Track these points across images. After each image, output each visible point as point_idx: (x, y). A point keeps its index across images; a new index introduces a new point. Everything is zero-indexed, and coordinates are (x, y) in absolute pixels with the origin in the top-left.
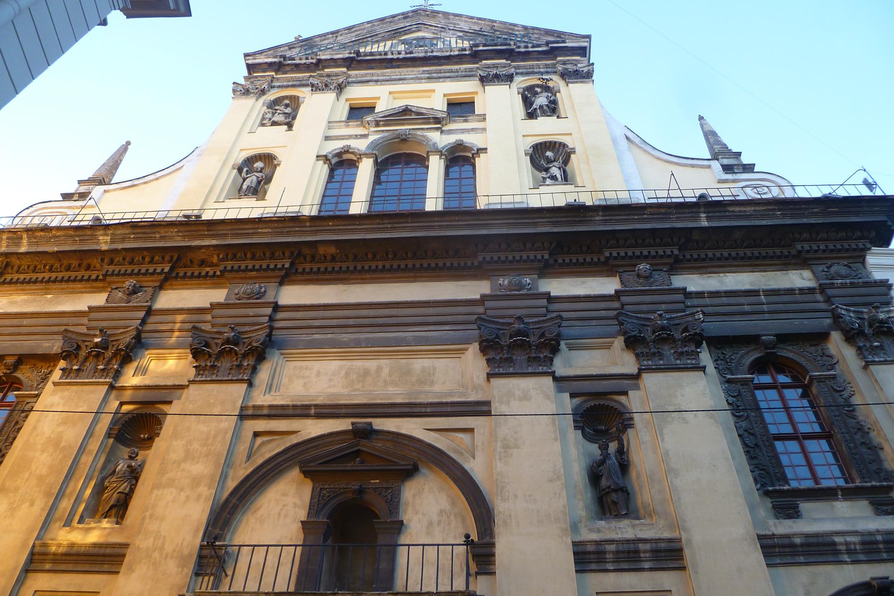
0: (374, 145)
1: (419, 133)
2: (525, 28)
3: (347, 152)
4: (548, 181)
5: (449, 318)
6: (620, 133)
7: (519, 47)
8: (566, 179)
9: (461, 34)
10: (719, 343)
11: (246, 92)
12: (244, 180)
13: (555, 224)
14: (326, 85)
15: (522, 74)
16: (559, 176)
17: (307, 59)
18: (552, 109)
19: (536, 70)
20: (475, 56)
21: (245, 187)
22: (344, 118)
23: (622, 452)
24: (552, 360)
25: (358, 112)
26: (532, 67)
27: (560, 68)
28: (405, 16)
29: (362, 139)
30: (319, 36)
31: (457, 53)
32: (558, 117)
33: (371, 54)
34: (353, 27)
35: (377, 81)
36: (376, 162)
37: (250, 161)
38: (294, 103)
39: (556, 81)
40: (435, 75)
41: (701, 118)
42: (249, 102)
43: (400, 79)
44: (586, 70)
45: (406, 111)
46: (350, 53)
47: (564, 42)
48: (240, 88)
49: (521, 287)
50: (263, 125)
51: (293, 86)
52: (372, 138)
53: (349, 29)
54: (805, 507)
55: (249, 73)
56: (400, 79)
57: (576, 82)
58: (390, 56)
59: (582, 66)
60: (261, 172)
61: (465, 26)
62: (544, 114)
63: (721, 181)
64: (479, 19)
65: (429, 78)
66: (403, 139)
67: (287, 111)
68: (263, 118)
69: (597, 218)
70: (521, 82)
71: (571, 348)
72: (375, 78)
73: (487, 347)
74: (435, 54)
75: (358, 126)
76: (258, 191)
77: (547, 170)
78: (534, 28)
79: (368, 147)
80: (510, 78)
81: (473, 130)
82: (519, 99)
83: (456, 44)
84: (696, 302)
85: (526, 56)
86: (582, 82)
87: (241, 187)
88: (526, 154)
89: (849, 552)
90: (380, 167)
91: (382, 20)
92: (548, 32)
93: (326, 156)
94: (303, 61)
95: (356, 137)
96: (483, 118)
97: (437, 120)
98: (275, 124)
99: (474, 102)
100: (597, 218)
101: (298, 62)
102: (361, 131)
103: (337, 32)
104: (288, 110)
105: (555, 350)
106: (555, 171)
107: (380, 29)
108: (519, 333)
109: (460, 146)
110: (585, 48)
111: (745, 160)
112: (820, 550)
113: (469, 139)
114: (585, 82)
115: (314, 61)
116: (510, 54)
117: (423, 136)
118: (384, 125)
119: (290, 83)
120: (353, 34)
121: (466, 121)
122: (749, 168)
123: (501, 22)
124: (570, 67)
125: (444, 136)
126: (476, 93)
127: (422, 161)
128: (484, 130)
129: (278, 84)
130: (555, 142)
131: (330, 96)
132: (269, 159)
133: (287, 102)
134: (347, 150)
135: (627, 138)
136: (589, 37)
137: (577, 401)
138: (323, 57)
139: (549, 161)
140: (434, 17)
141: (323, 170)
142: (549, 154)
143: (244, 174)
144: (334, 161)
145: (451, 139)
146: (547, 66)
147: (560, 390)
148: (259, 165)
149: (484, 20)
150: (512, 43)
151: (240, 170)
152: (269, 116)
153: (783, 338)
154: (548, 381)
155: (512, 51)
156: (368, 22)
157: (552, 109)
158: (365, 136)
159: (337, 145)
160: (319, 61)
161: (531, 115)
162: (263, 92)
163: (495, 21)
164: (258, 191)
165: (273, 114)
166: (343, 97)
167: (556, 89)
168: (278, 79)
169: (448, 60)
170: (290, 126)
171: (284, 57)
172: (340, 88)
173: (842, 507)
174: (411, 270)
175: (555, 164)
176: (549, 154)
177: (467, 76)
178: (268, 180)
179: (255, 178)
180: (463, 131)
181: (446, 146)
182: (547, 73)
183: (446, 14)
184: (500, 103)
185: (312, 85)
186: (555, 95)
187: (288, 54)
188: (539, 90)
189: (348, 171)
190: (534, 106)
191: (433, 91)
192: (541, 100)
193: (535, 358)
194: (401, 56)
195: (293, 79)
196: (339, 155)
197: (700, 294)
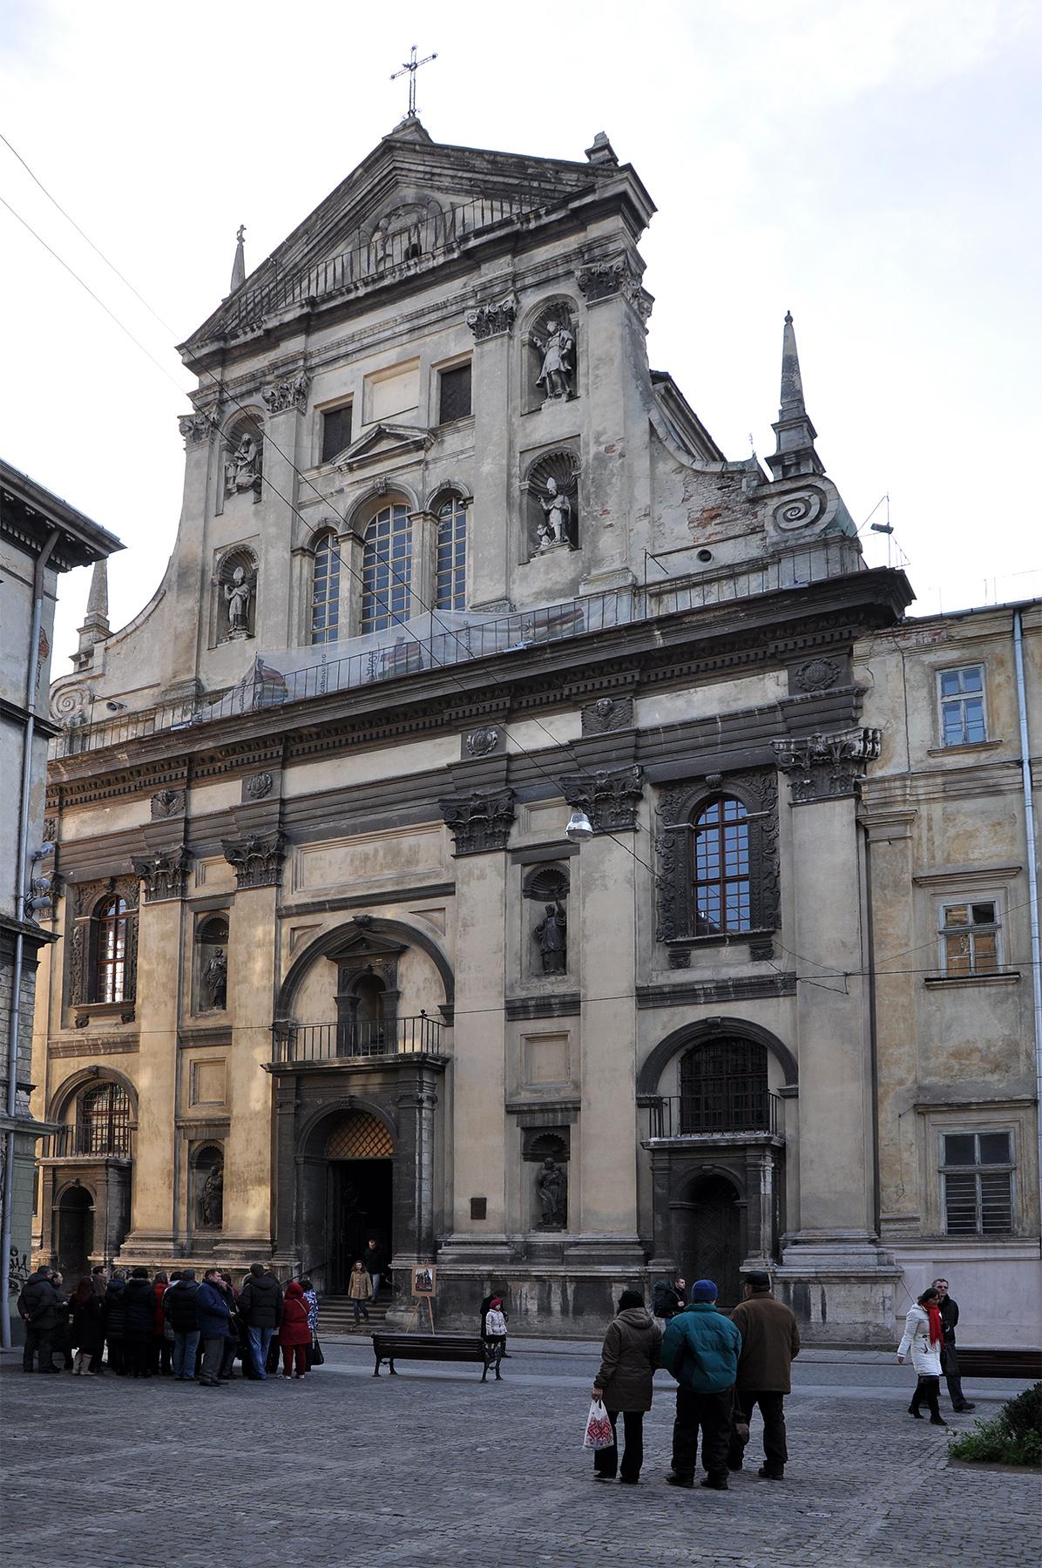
4: (545, 541)
5: (425, 792)
10: (663, 786)
23: (562, 914)
24: (507, 834)
28: (369, 165)
49: (484, 745)
54: (696, 954)
71: (531, 809)
73: (452, 826)
74: (412, 272)
84: (650, 740)
89: (705, 995)
97: (419, 446)
105: (510, 820)
106: (556, 519)
108: (475, 811)
112: (685, 995)
137: (528, 869)
145: (435, 479)
147: (514, 862)
153: (726, 774)
154: (501, 856)
173: (726, 952)
174: (391, 735)
175: (558, 502)
193: (492, 834)
197: (655, 730)
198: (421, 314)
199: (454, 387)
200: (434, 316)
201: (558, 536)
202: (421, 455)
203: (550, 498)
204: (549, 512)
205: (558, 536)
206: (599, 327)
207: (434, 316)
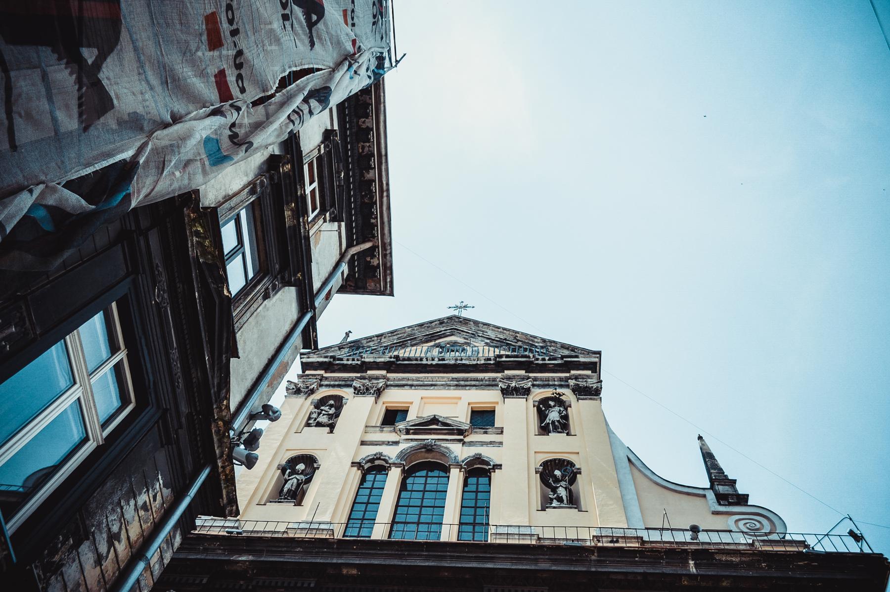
0: (402, 455)
1: (444, 444)
2: (544, 341)
3: (379, 459)
4: (555, 503)
6: (622, 455)
7: (537, 359)
8: (573, 501)
9: (488, 341)
11: (298, 391)
12: (286, 481)
13: (554, 561)
14: (367, 389)
15: (538, 386)
16: (564, 498)
17: (353, 360)
18: (563, 426)
19: (551, 383)
20: (499, 366)
21: (285, 490)
22: (379, 424)
25: (392, 417)
26: (548, 379)
27: (572, 382)
28: (441, 322)
29: (394, 446)
30: (366, 338)
31: (483, 362)
32: (568, 434)
33: (409, 359)
34: (396, 331)
35: (411, 386)
36: (403, 471)
37: (293, 462)
38: (338, 403)
39: (568, 395)
40: (462, 383)
41: (700, 438)
42: (299, 400)
43: (432, 385)
44: (595, 386)
45: (434, 420)
46: (391, 357)
47: (577, 357)
48: (292, 386)
50: (308, 425)
51: (339, 386)
52: (403, 446)
53: (392, 332)
55: (304, 372)
56: (432, 385)
57: (586, 399)
58: (424, 362)
59: (592, 383)
60: (301, 473)
61: (492, 335)
62: (555, 429)
63: (716, 513)
64: (504, 329)
65: (457, 385)
66: (429, 449)
67: (331, 412)
68: (309, 418)
69: (593, 558)
70: (539, 394)
72: (410, 383)
74: (464, 362)
75: (391, 432)
76: (297, 496)
77: (554, 490)
78: (551, 342)
79: (398, 457)
80: (526, 392)
81: (491, 443)
82: (533, 412)
83: (484, 352)
85: (543, 368)
86: (591, 399)
87: (282, 490)
88: (536, 472)
90: (407, 473)
91: (421, 325)
92: (564, 346)
93: (359, 463)
94: (350, 362)
95: (388, 443)
96: (501, 431)
97: (461, 432)
98: (319, 425)
99: (494, 411)
100: (593, 558)
101: (345, 362)
102: (393, 437)
103: (381, 335)
104: (332, 411)
106: (562, 492)
107: (419, 334)
109: (478, 459)
110: (596, 363)
111: (741, 489)
113: (487, 453)
114: (594, 399)
115: (359, 363)
116: (529, 366)
117: (446, 448)
118: (414, 434)
119: (337, 383)
120: (395, 337)
121: (486, 433)
122: (743, 500)
123: (523, 334)
124: (582, 384)
125: (465, 448)
126: (497, 403)
127: (446, 469)
128: (501, 443)
129: (326, 383)
130: (564, 460)
131: (370, 399)
132: (310, 461)
133: (332, 402)
134: (379, 457)
135: (629, 460)
136: (599, 353)
138: (367, 360)
139: (557, 480)
140: (466, 324)
141: (357, 474)
142: (557, 473)
143: (286, 476)
144: (366, 467)
146: (561, 379)
148: (301, 467)
149: (509, 330)
150: (531, 355)
151: (283, 470)
152: (315, 416)
155: (532, 362)
156: (409, 327)
157: (563, 426)
158: (396, 443)
159: (370, 451)
160: (363, 363)
161: (544, 430)
162: (312, 392)
163: (518, 333)
164: (297, 496)
165: (319, 414)
166: (381, 401)
167: (567, 404)
168: (326, 378)
169: (476, 368)
170: (332, 427)
171: (333, 357)
172: (379, 393)
175: (563, 483)
176: (557, 473)
177: (492, 384)
178: (308, 481)
179: (295, 481)
180: (483, 444)
181: (466, 459)
182: (561, 386)
183: (476, 323)
184: (517, 414)
185: (355, 389)
186: (566, 409)
187: (338, 354)
188: (552, 403)
189: (379, 477)
190: (547, 421)
191: (460, 398)
192: (554, 415)
194: (434, 363)
195: (339, 379)
196: (372, 461)
198: (466, 380)
199: (483, 418)
200: (473, 383)
201: (565, 502)
202: (461, 437)
203: (557, 480)
204: (558, 487)
205: (565, 502)
206: (579, 409)
207: (473, 383)
